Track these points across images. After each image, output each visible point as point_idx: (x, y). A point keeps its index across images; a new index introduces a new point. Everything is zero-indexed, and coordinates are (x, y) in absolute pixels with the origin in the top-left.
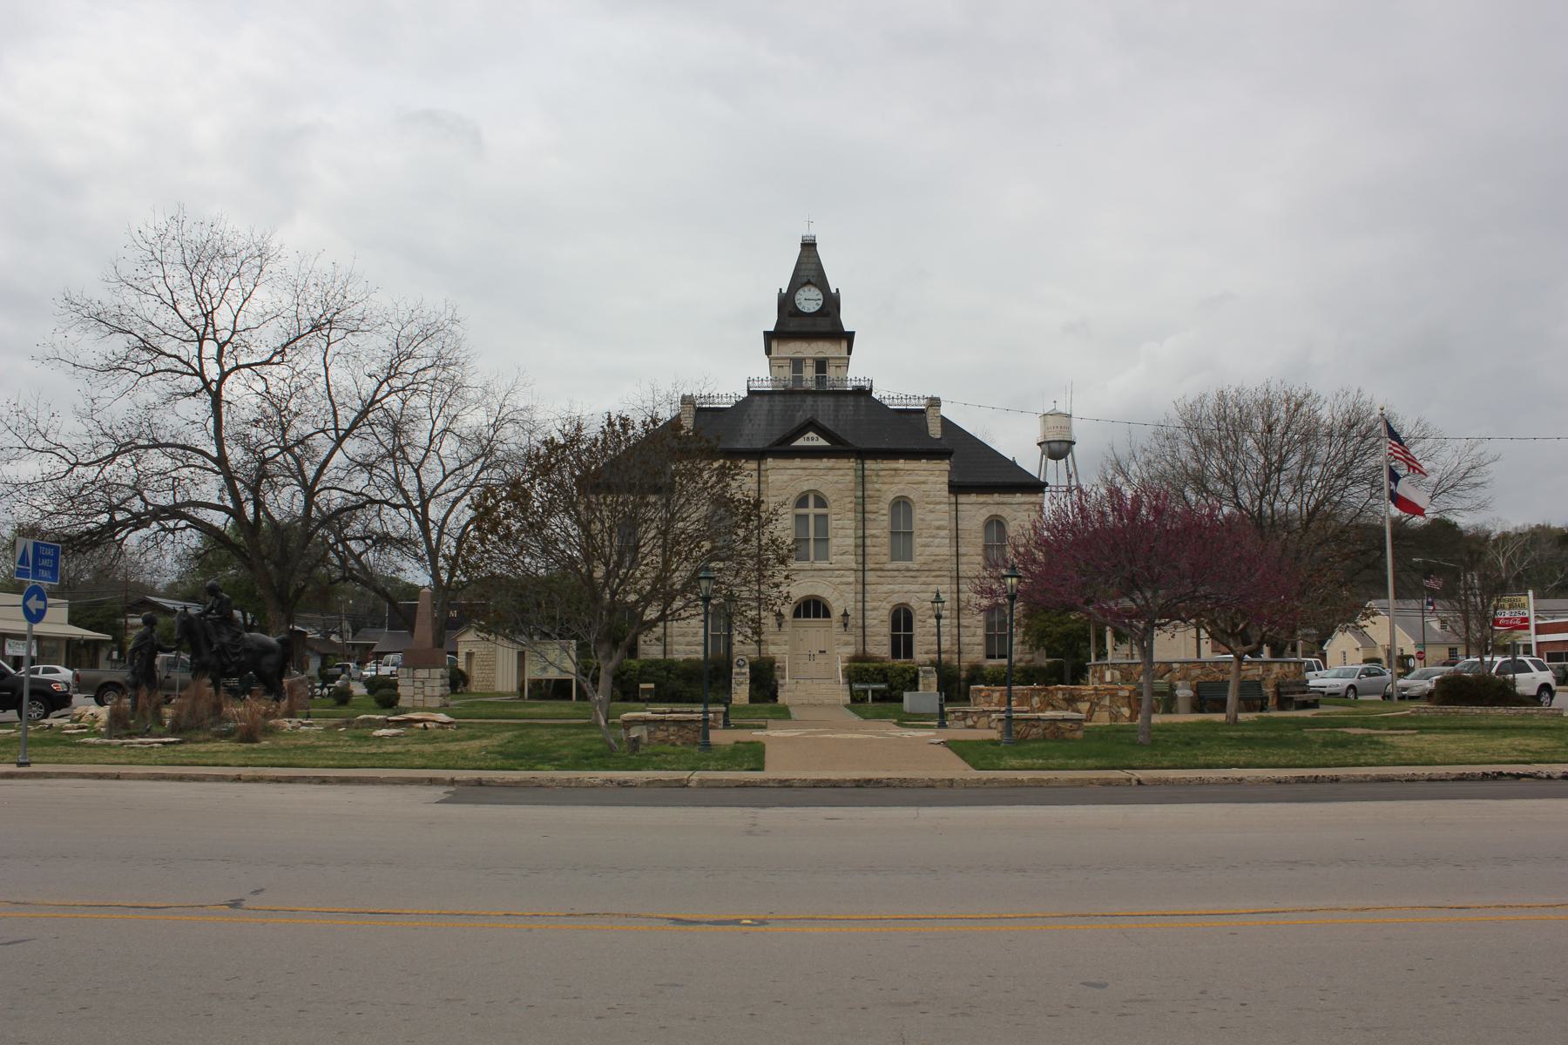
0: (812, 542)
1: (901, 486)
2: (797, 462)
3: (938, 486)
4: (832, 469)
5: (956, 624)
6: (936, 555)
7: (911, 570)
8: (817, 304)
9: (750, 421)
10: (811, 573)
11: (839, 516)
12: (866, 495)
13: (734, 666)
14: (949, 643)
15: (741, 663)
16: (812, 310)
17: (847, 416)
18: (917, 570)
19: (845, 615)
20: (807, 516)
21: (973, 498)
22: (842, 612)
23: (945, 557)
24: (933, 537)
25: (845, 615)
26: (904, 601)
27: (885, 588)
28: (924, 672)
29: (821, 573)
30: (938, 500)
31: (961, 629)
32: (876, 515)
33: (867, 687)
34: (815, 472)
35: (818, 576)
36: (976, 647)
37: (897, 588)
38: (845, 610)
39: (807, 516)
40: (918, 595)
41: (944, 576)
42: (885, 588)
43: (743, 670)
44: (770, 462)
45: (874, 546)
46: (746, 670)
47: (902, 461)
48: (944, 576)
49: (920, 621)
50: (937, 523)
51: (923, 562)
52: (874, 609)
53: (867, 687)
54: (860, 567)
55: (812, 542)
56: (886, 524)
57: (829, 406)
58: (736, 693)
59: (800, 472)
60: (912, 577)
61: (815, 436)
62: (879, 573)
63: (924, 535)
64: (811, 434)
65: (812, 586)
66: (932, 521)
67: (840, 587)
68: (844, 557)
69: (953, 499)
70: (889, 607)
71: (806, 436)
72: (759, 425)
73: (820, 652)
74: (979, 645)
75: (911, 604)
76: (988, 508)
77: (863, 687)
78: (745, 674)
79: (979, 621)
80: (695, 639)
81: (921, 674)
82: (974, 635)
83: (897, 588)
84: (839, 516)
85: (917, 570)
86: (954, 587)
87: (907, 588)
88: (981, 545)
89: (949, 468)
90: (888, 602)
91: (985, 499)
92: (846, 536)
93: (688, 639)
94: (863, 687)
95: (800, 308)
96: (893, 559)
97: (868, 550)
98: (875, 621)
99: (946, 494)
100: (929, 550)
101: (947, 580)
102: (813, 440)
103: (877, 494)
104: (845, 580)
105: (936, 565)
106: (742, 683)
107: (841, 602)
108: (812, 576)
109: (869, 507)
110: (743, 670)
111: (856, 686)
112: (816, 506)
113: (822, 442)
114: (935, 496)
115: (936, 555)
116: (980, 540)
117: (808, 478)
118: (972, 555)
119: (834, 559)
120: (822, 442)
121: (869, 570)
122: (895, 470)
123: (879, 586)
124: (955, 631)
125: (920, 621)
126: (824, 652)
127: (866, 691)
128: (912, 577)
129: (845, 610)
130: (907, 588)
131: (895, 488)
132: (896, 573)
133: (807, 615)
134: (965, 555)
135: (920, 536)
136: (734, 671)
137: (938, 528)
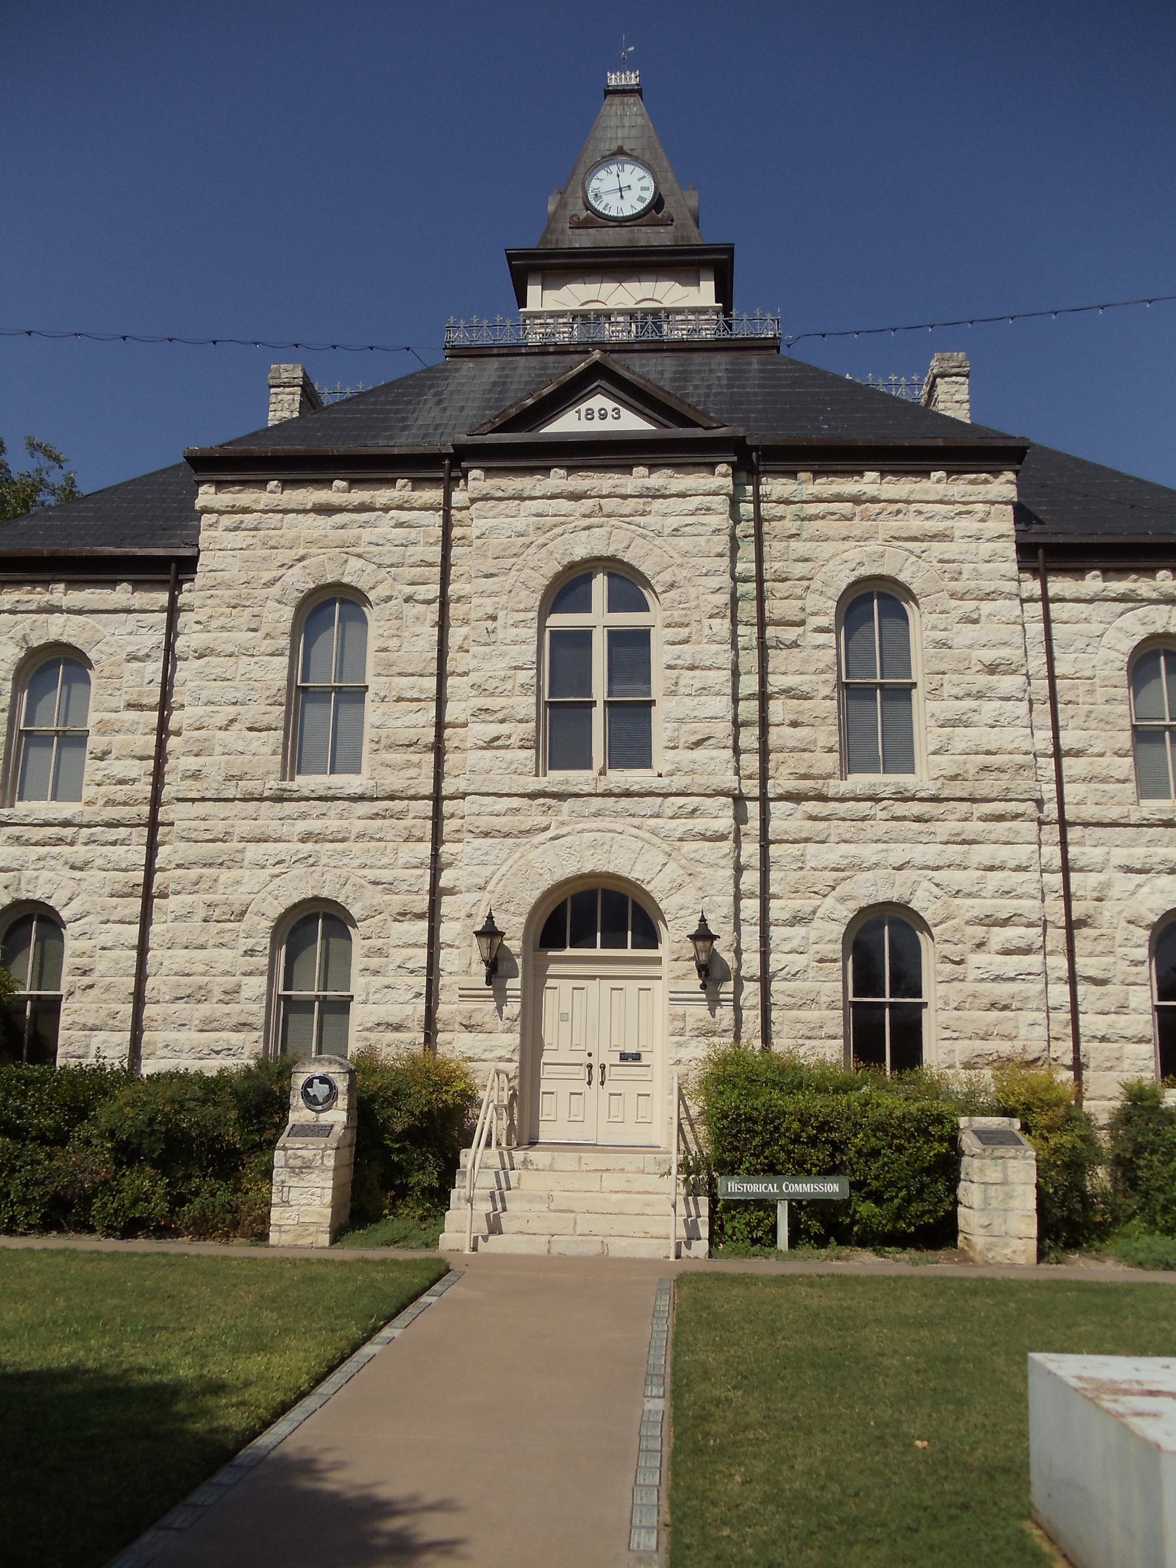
0: (598, 715)
1: (872, 547)
2: (558, 480)
3: (985, 548)
4: (658, 495)
5: (1065, 974)
6: (988, 753)
7: (913, 799)
8: (641, 199)
9: (439, 402)
10: (597, 802)
11: (683, 632)
12: (767, 575)
13: (297, 1100)
14: (1040, 1031)
15: (319, 1090)
16: (628, 212)
17: (709, 387)
18: (935, 799)
19: (703, 935)
20: (583, 638)
21: (1093, 583)
22: (693, 928)
23: (1020, 759)
24: (980, 696)
25: (703, 935)
26: (893, 895)
27: (834, 854)
28: (986, 1137)
29: (625, 802)
30: (988, 586)
31: (1081, 989)
32: (800, 630)
33: (773, 1189)
34: (609, 504)
35: (617, 814)
36: (1131, 1048)
37: (869, 852)
38: (703, 920)
39: (583, 638)
40: (937, 875)
41: (1016, 817)
42: (834, 854)
43: (327, 1118)
44: (477, 480)
45: (794, 724)
46: (338, 1116)
47: (871, 476)
48: (1016, 817)
49: (946, 959)
50: (989, 656)
51: (949, 772)
52: (797, 920)
53: (773, 1189)
54: (751, 787)
55: (598, 715)
56: (829, 656)
57: (662, 372)
58: (286, 1203)
59: (564, 505)
60: (918, 819)
61: (609, 404)
62: (811, 807)
63: (948, 690)
64: (599, 402)
65: (594, 845)
66: (971, 647)
67: (688, 847)
68: (700, 754)
69: (1032, 586)
70: (846, 912)
71: (583, 407)
72: (462, 408)
73: (624, 1057)
74: (1141, 1041)
75: (915, 905)
76: (1141, 612)
77: (756, 1188)
78: (327, 1130)
79: (1136, 963)
80: (226, 1009)
81: (968, 1141)
82: (1122, 1009)
83: (869, 852)
84: (683, 632)
85: (935, 799)
86: (1052, 853)
87: (899, 852)
88: (1126, 723)
89: (1011, 492)
90: (842, 900)
91: (1132, 586)
92: (703, 690)
93: (205, 1009)
94: (756, 1188)
95: (600, 208)
96: (849, 765)
97: (774, 734)
98: (800, 961)
99: (1012, 568)
100: (962, 738)
101: (1028, 829)
102: (603, 417)
103: (800, 569)
104: (699, 824)
105: (989, 785)
106: (307, 1166)
107: (688, 896)
108: (597, 814)
109: (775, 608)
110: (327, 1118)
111: (733, 1187)
112: (615, 605)
113: (631, 423)
114: (978, 575)
115: (988, 753)
116: (1124, 709)
117: (587, 522)
118: (1102, 755)
119: (661, 758)
120: (631, 423)
121: (780, 798)
122: (856, 500)
123: (811, 848)
124: (1060, 993)
125: (946, 959)
126: (637, 1057)
127: (766, 1205)
128: (918, 819)
129: (703, 920)
130: (899, 852)
131: (854, 553)
132: (864, 807)
133: (583, 939)
134: (1078, 753)
135: (935, 692)
136: (294, 1117)
137: (992, 669)
